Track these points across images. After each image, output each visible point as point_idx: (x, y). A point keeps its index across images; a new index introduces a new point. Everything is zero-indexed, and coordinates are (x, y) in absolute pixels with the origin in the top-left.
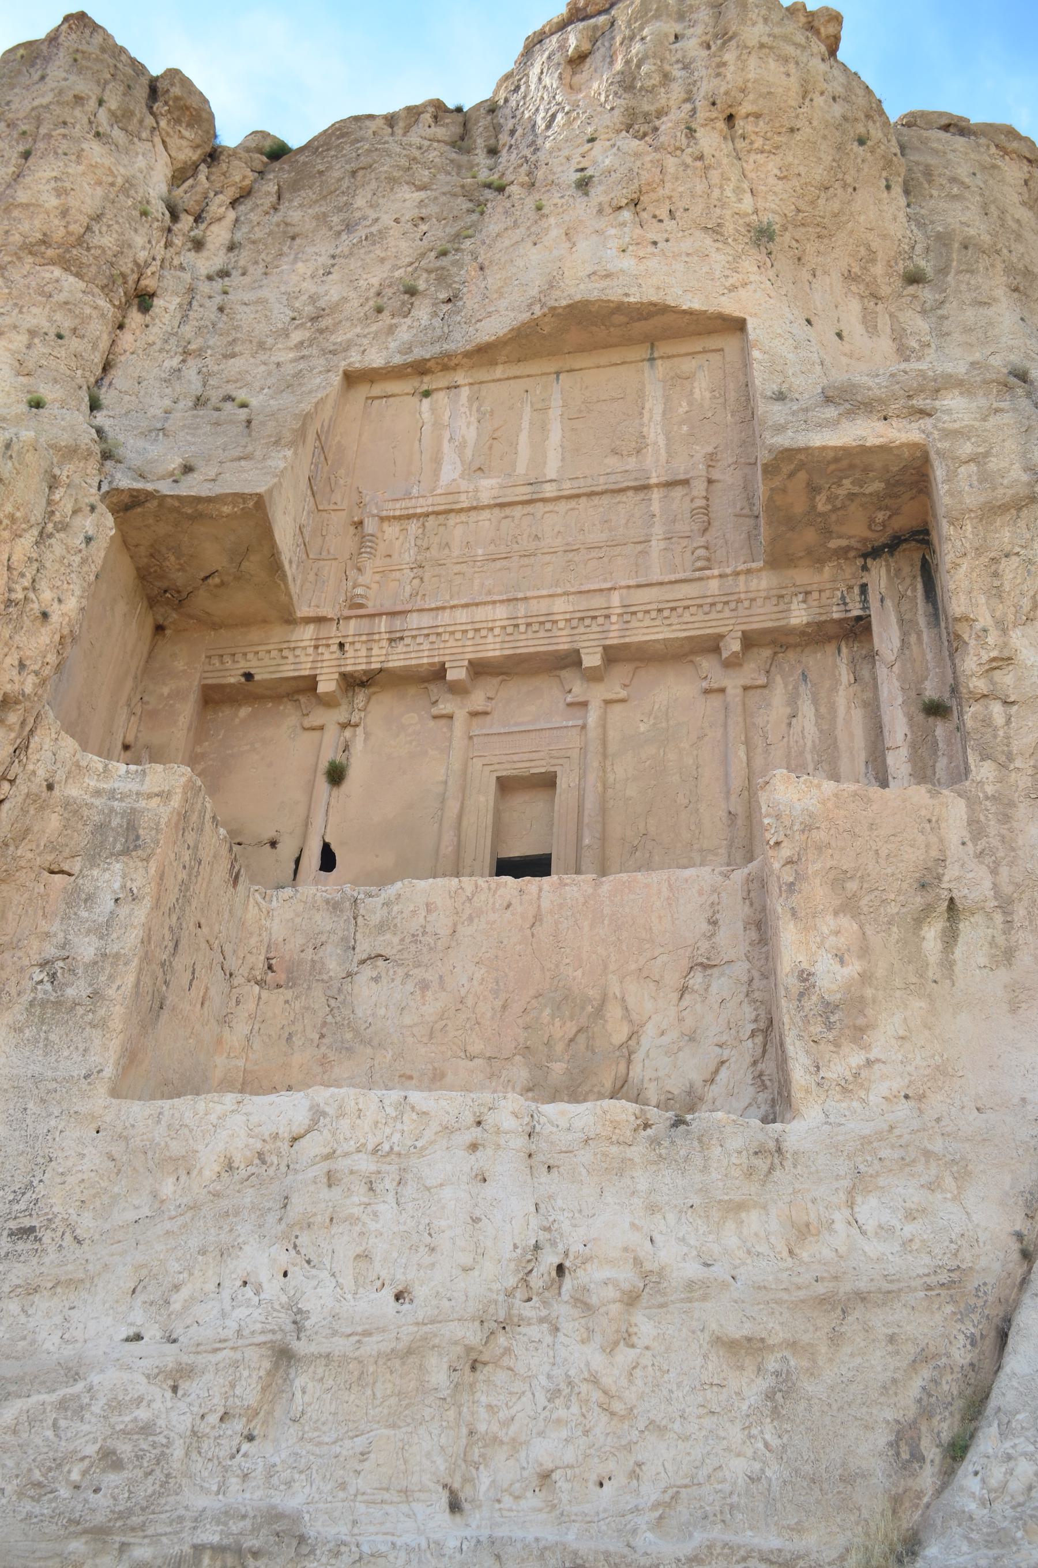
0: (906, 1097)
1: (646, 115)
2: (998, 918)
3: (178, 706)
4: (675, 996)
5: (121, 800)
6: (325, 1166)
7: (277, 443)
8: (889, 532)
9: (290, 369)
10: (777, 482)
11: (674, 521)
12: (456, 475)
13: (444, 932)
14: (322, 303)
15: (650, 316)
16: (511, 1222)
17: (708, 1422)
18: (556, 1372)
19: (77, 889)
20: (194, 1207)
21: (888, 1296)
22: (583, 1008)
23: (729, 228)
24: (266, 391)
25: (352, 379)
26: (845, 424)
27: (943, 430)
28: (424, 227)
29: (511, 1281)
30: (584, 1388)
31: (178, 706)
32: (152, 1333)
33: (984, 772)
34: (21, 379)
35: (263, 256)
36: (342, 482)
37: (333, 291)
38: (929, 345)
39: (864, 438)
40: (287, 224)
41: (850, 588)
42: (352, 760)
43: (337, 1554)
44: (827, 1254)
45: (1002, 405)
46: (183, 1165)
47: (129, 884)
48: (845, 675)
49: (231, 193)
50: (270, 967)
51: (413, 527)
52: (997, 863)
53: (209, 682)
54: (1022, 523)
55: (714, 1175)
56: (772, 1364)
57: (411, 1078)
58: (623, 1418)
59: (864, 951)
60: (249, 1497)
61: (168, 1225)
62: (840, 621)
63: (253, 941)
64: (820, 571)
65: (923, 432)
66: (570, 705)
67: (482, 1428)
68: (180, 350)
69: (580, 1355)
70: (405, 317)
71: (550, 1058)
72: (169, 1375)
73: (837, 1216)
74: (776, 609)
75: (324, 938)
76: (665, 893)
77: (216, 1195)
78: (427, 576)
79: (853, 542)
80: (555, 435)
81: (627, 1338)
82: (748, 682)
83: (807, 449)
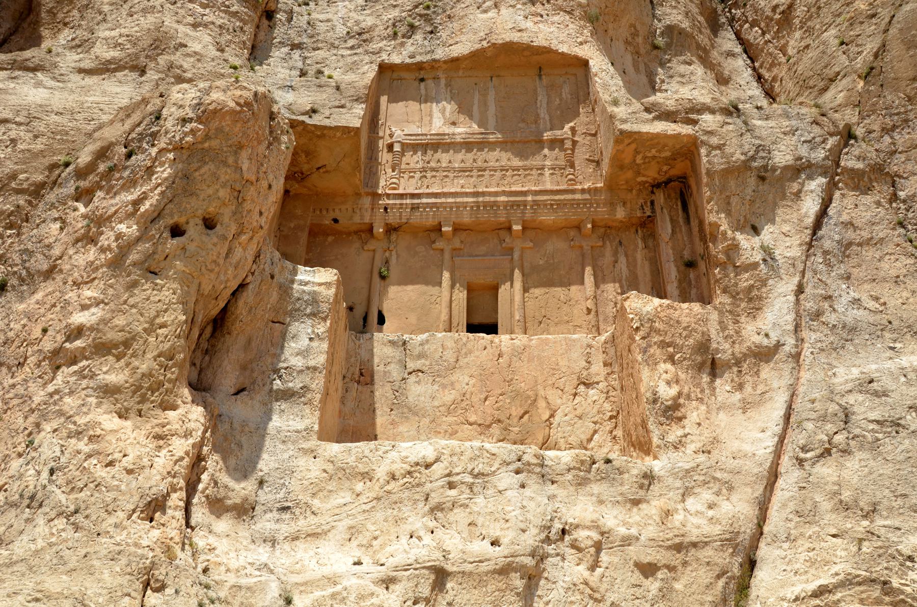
0: (703, 452)
4: (572, 397)
7: (356, 100)
8: (667, 176)
9: (349, 60)
10: (621, 147)
13: (452, 360)
14: (363, 25)
15: (543, 53)
18: (567, 579)
20: (378, 499)
22: (526, 401)
26: (656, 123)
30: (582, 586)
32: (366, 560)
37: (369, 21)
41: (646, 203)
44: (677, 524)
47: (316, 330)
50: (361, 374)
52: (734, 342)
53: (314, 222)
56: (660, 575)
57: (440, 433)
58: (600, 601)
59: (677, 382)
61: (364, 507)
62: (640, 218)
63: (353, 360)
72: (383, 581)
77: (389, 492)
79: (649, 180)
82: (594, 244)
83: (639, 132)
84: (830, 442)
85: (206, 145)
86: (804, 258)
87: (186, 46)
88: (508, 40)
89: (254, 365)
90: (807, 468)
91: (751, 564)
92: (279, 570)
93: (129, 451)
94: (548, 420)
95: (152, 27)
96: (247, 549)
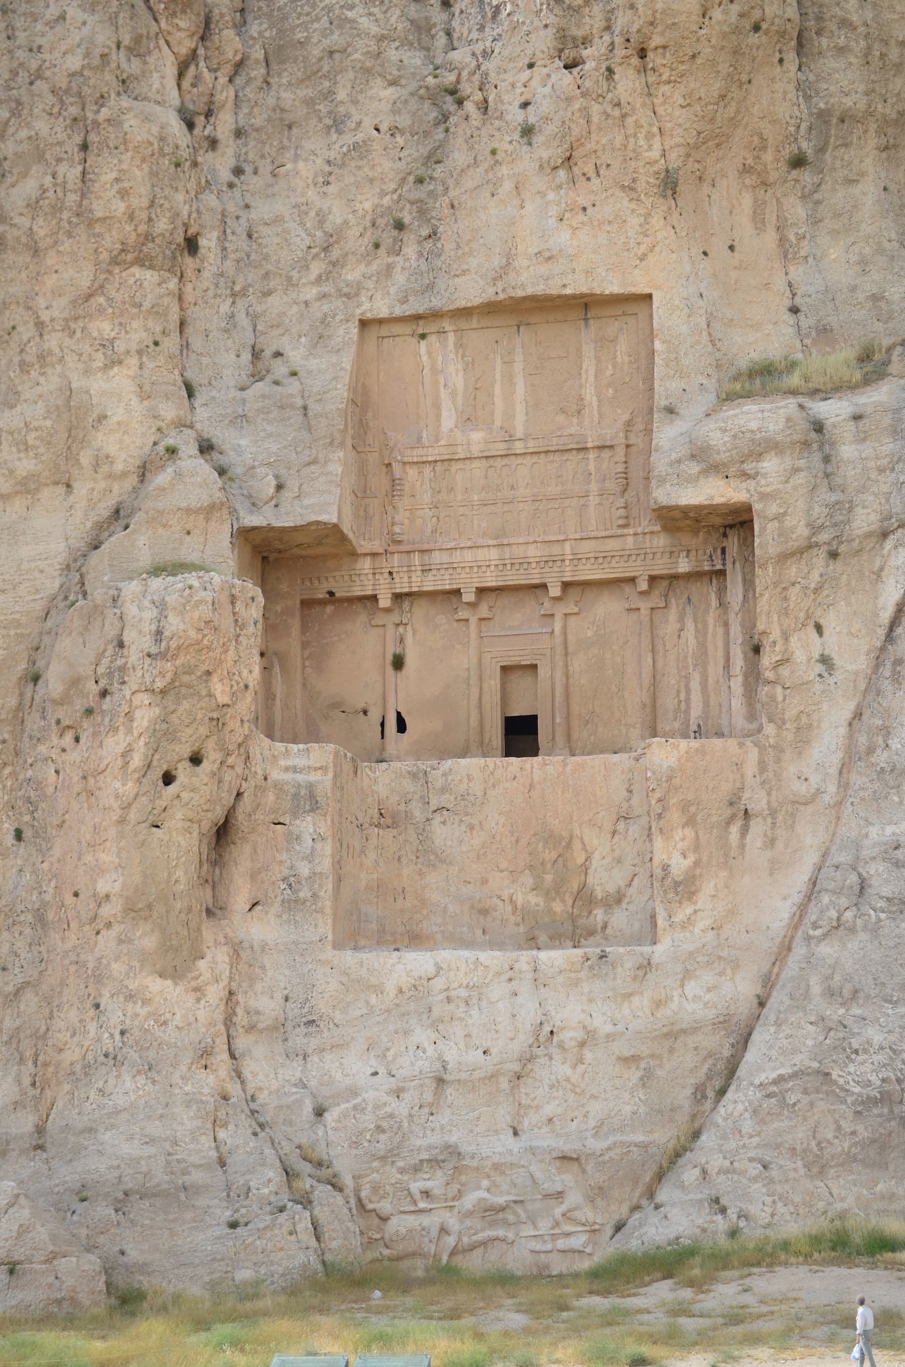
1: (574, 39)
2: (769, 820)
3: (289, 621)
4: (610, 836)
5: (300, 772)
6: (445, 994)
7: (331, 443)
11: (604, 480)
12: (452, 426)
13: (480, 794)
14: (329, 227)
16: (529, 1013)
17: (616, 1092)
18: (553, 1077)
19: (290, 833)
20: (388, 1011)
21: (695, 1030)
23: (641, 185)
24: (303, 339)
25: (364, 324)
27: (760, 493)
28: (400, 140)
29: (531, 1040)
30: (564, 1083)
31: (289, 621)
32: (382, 1071)
33: (770, 729)
34: (146, 403)
35: (267, 148)
36: (371, 424)
38: (804, 237)
39: (712, 498)
40: (282, 110)
42: (407, 650)
43: (473, 1158)
44: (669, 1012)
45: (802, 463)
46: (378, 989)
48: (714, 602)
49: (228, 69)
51: (427, 470)
53: (305, 597)
54: (803, 562)
55: (619, 981)
60: (435, 1139)
61: (378, 1019)
63: (370, 800)
64: (697, 536)
65: (749, 491)
66: (544, 615)
67: (524, 1102)
68: (228, 292)
69: (563, 1070)
70: (398, 255)
71: (544, 872)
72: (395, 1092)
73: (676, 993)
74: (669, 561)
75: (410, 797)
76: (603, 772)
77: (398, 1005)
78: (442, 515)
80: (518, 367)
81: (580, 1061)
84: (838, 919)
85: (177, 684)
86: (869, 671)
87: (106, 417)
88: (530, 291)
89: (263, 874)
90: (813, 946)
91: (746, 1039)
92: (313, 1083)
93: (176, 1010)
94: (584, 864)
95: (60, 402)
96: (283, 1065)
